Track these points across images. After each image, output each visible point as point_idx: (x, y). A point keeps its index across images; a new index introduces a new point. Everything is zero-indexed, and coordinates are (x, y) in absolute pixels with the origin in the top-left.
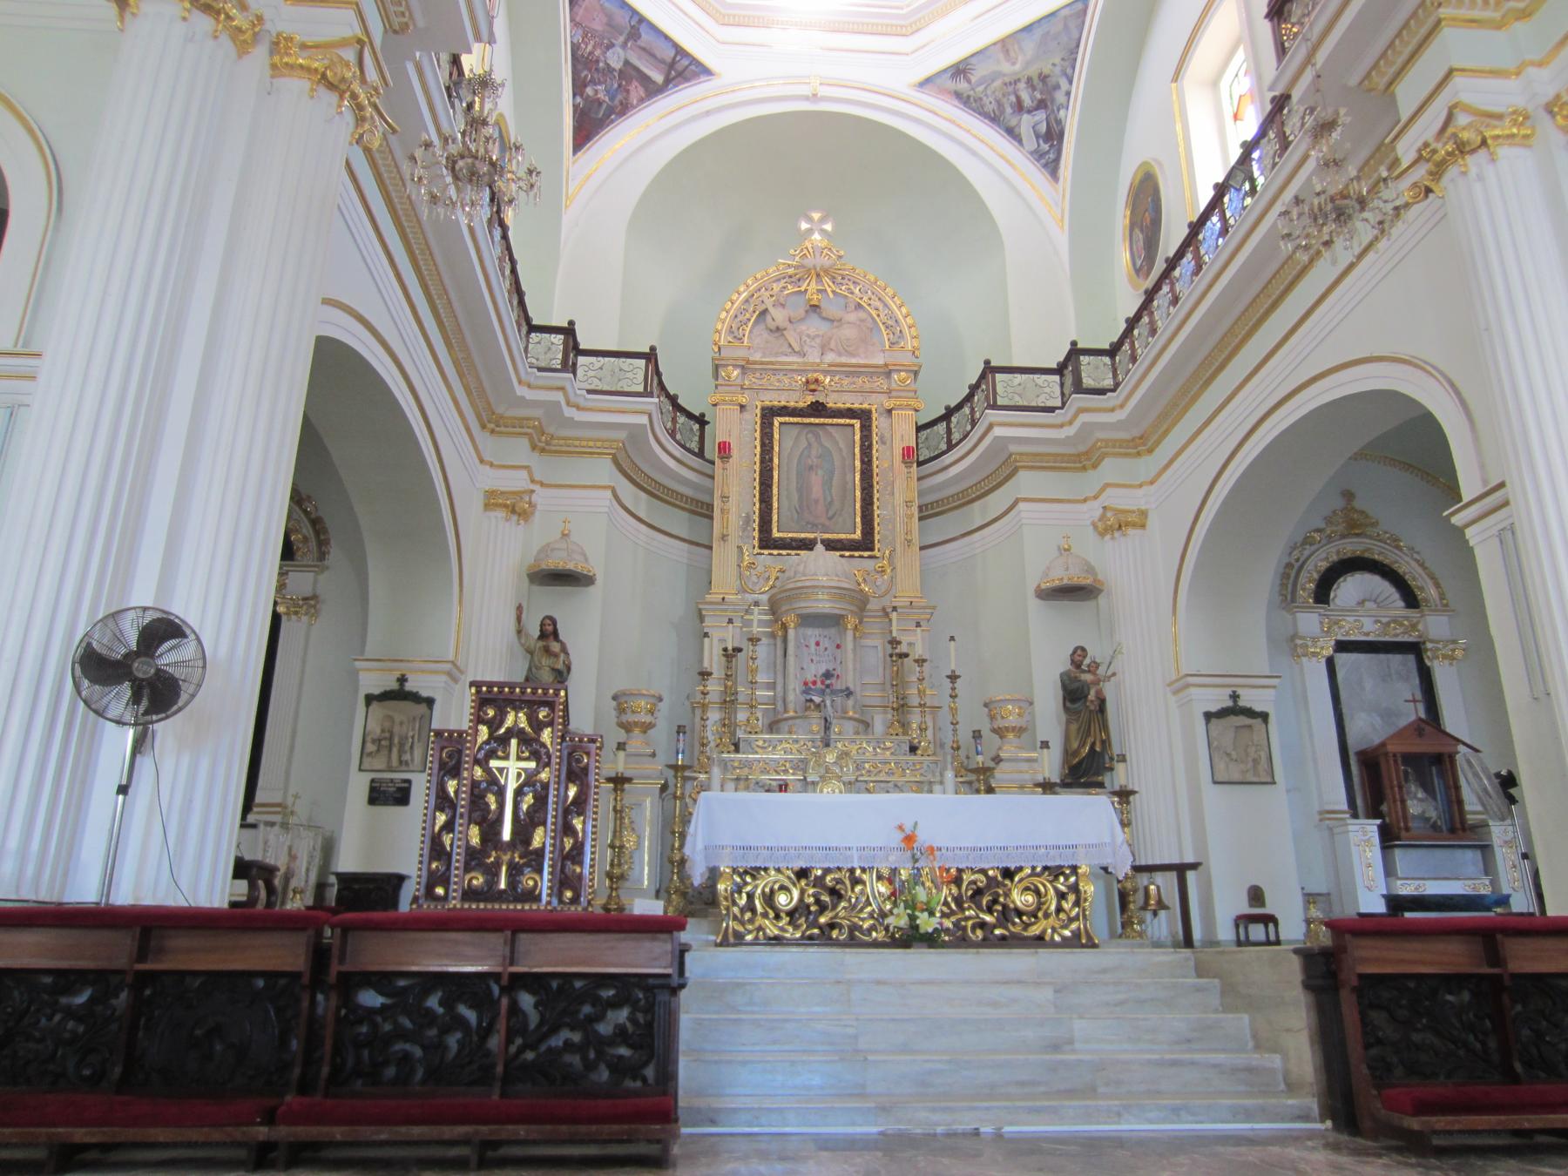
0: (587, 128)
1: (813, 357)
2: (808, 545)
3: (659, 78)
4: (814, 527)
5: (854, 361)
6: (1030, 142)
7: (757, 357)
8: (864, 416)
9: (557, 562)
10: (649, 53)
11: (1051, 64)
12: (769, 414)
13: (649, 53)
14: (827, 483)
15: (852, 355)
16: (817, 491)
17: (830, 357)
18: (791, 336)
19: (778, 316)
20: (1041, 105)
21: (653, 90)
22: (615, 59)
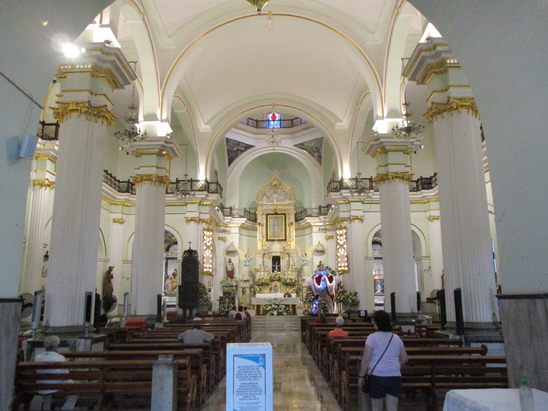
0: (230, 161)
1: (275, 203)
2: (274, 240)
3: (243, 149)
4: (276, 237)
5: (283, 203)
6: (316, 158)
7: (265, 203)
8: (285, 214)
9: (231, 249)
10: (242, 146)
11: (318, 145)
12: (267, 215)
13: (242, 146)
14: (278, 228)
15: (283, 201)
16: (276, 230)
17: (278, 203)
18: (271, 198)
19: (269, 194)
20: (318, 152)
21: (242, 151)
22: (235, 149)
